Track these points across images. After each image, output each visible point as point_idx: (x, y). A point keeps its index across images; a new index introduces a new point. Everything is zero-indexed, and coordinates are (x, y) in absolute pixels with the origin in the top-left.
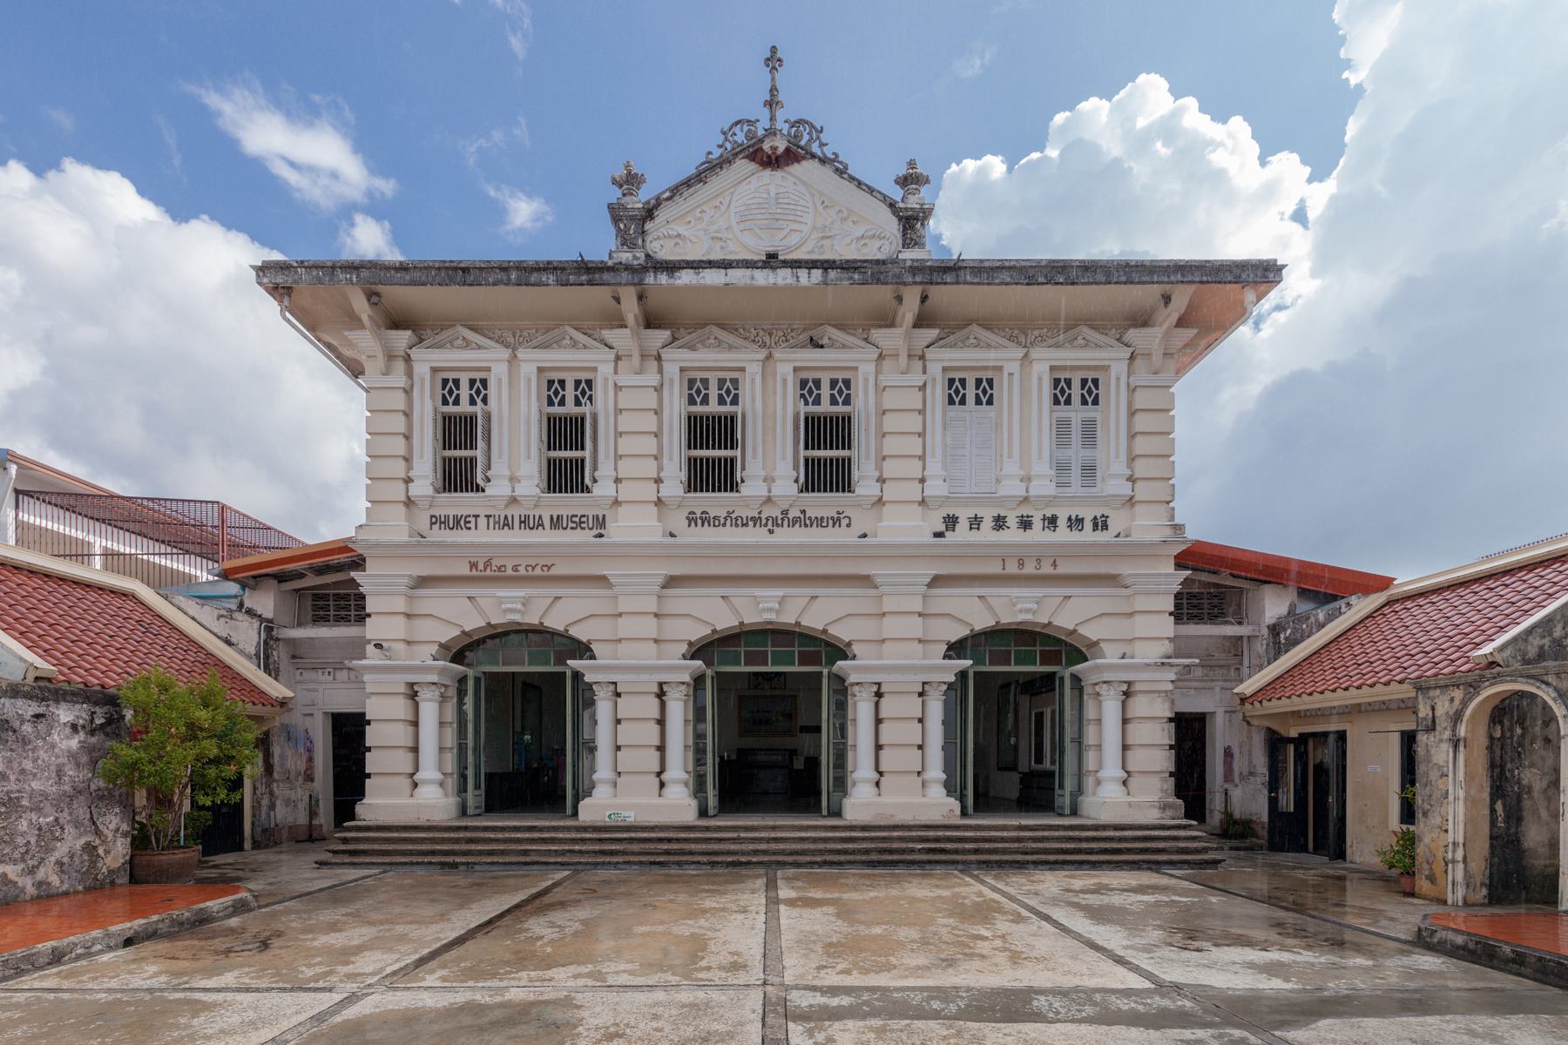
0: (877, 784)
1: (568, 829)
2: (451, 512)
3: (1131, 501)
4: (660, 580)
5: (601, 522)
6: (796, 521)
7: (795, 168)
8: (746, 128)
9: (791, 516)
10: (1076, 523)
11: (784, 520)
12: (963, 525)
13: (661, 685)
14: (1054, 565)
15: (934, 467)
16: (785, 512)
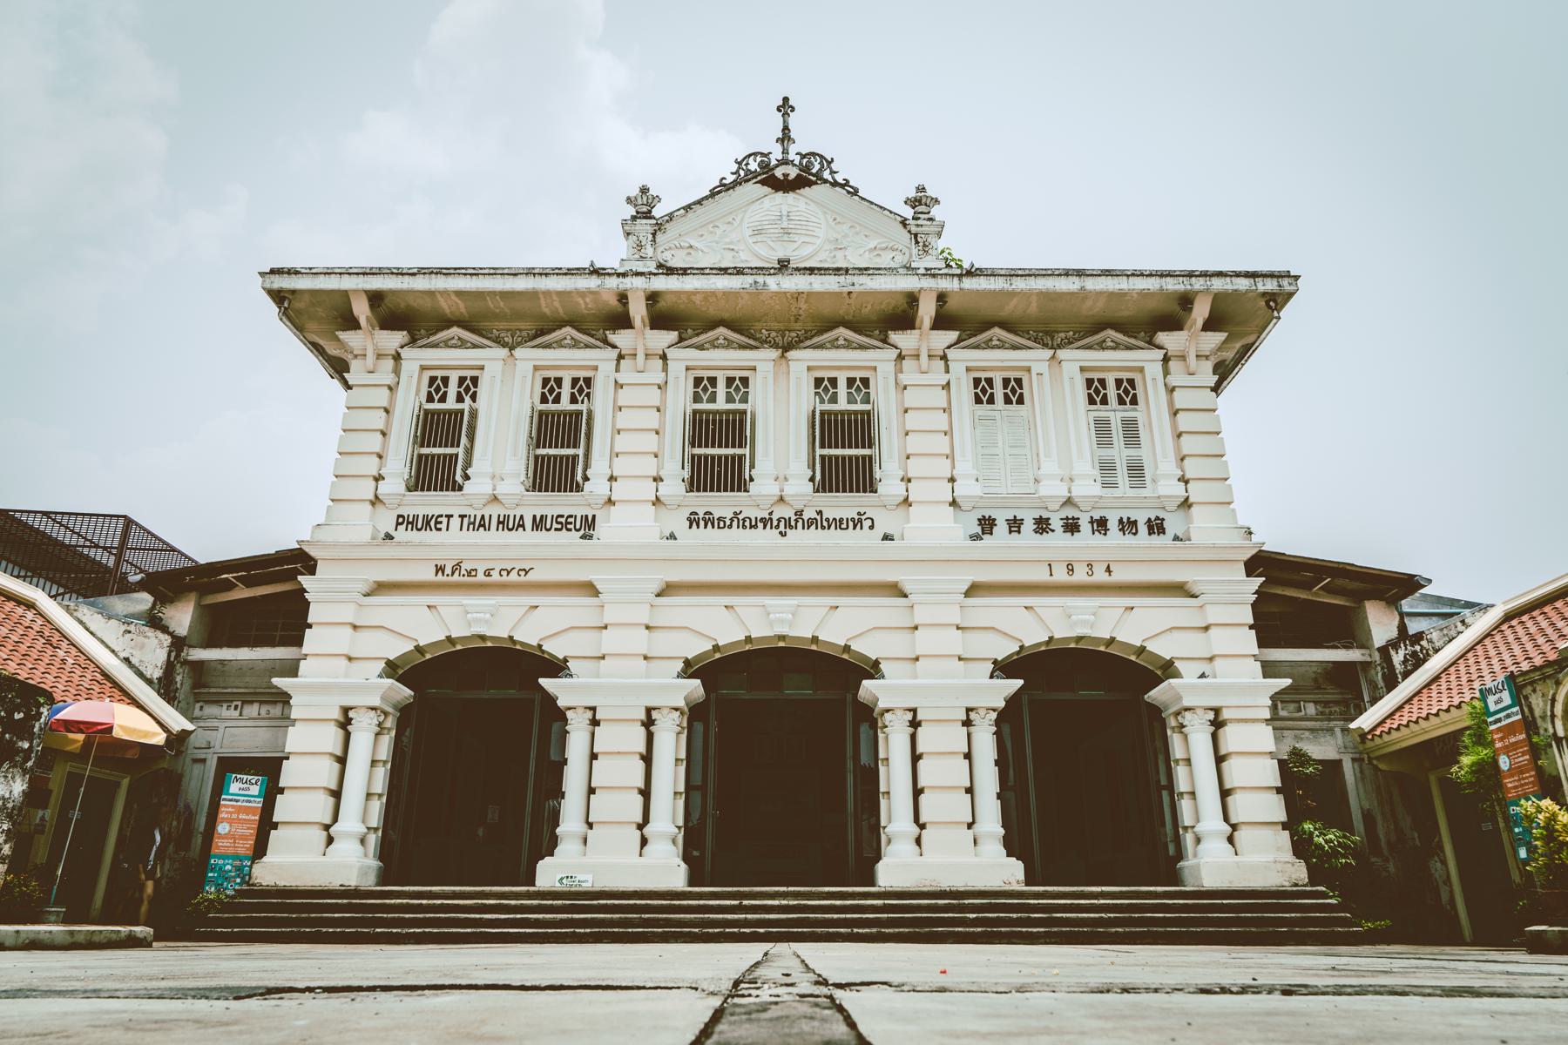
0: (918, 841)
1: (529, 896)
2: (421, 511)
3: (1186, 504)
4: (656, 587)
5: (589, 523)
6: (811, 523)
7: (806, 191)
8: (759, 159)
9: (806, 517)
10: (1128, 526)
11: (798, 521)
12: (1001, 528)
13: (649, 710)
14: (1108, 570)
15: (964, 467)
16: (799, 513)
